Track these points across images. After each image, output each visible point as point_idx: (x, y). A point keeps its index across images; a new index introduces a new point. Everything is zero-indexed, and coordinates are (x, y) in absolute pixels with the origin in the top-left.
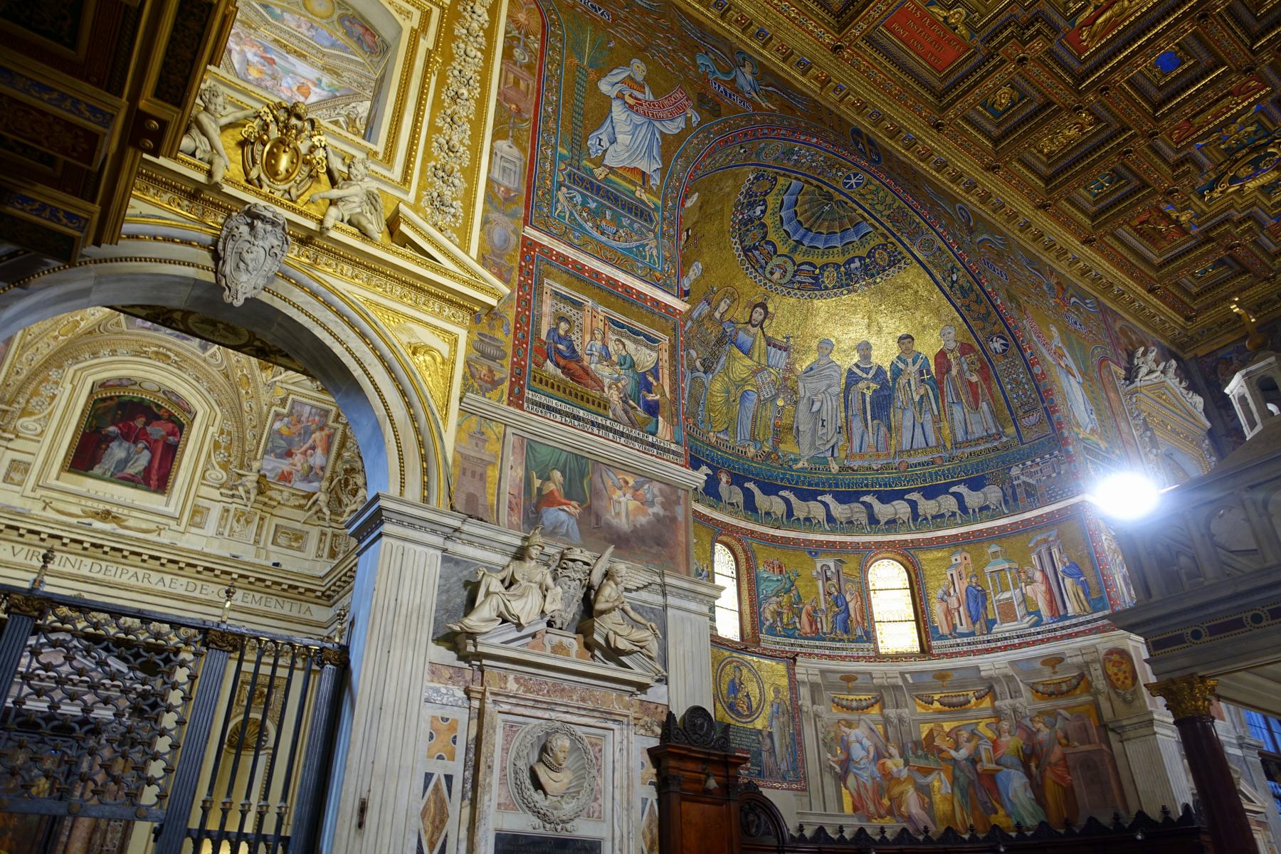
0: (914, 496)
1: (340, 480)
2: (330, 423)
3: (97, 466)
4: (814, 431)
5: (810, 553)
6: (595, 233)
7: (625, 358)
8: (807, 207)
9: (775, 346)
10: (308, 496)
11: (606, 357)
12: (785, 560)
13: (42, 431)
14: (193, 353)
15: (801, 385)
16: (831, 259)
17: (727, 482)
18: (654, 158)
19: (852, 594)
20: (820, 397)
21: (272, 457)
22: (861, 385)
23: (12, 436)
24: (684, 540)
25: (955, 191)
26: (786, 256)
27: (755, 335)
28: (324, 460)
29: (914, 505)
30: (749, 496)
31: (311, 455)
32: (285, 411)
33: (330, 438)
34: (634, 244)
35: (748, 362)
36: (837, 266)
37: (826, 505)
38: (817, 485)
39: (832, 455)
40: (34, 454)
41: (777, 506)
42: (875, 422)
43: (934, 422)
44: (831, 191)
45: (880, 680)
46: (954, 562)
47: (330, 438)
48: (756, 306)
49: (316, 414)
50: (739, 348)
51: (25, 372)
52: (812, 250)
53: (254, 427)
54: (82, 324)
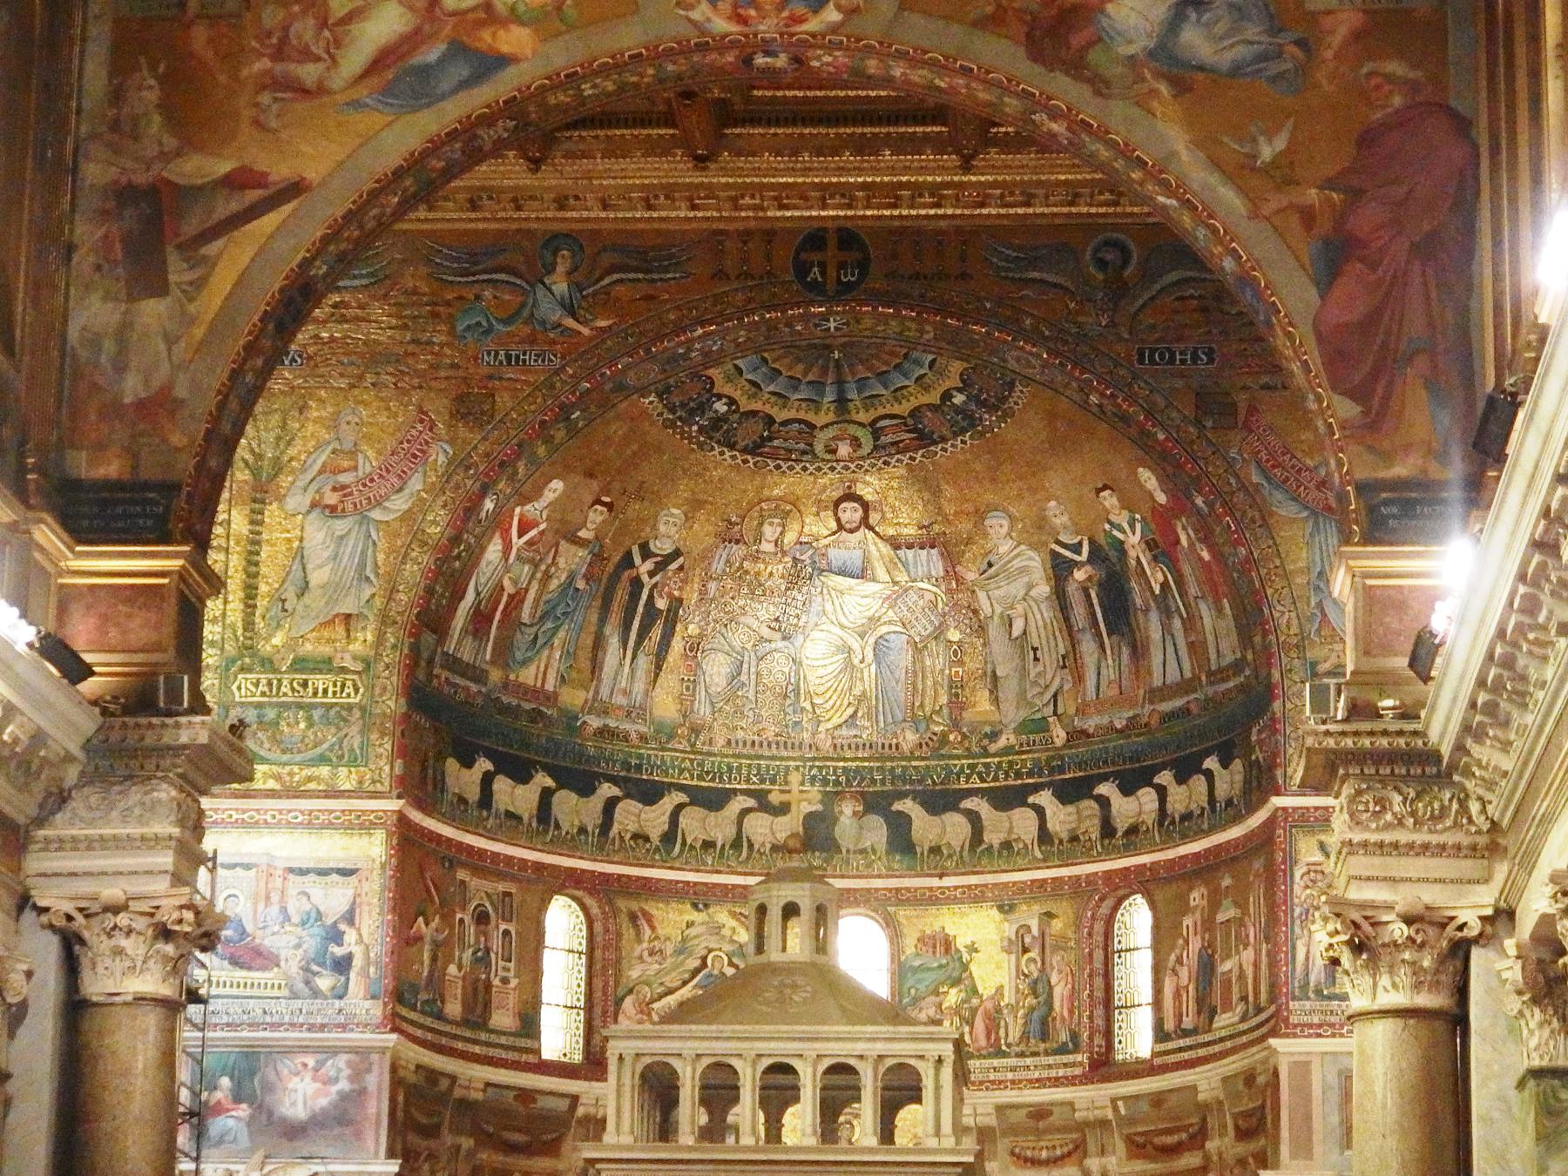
0: (1165, 778)
4: (1023, 672)
5: (1001, 908)
6: (276, 755)
7: (308, 914)
8: (801, 367)
9: (910, 547)
11: (287, 918)
12: (950, 931)
15: (981, 595)
16: (914, 403)
17: (855, 813)
18: (367, 578)
19: (1060, 972)
20: (1020, 608)
22: (1080, 575)
24: (374, 1110)
25: (1089, 215)
29: (1162, 792)
34: (325, 746)
35: (870, 587)
37: (1040, 811)
38: (1030, 774)
39: (1055, 713)
41: (954, 828)
42: (1114, 637)
43: (1185, 630)
45: (1084, 1114)
46: (1192, 903)
48: (837, 504)
50: (842, 572)
52: (876, 401)
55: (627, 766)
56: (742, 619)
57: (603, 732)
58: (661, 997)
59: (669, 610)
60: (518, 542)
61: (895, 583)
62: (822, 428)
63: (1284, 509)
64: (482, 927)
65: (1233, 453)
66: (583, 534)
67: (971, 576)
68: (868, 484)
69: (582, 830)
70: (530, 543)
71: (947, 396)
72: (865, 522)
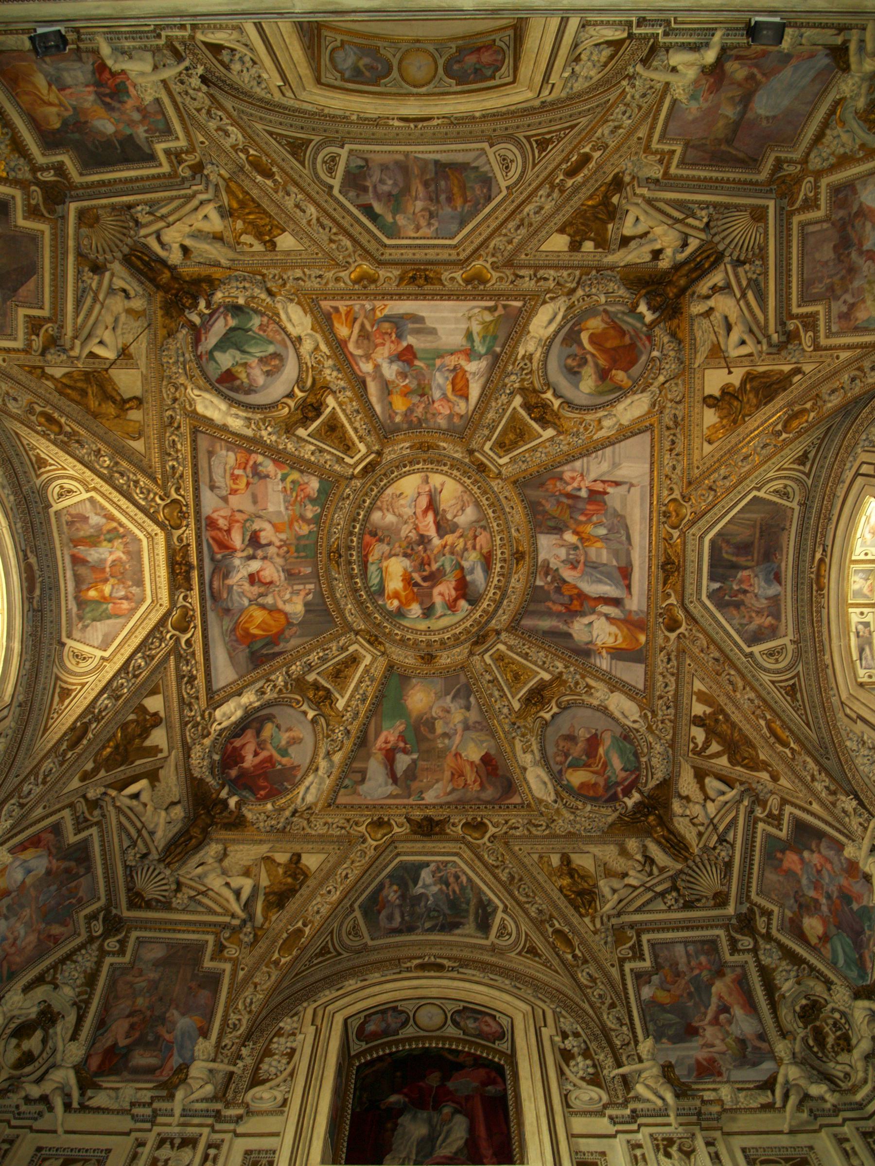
1: (805, 1040)
2: (728, 957)
3: (388, 1157)
10: (769, 1085)
13: (285, 1101)
14: (474, 946)
21: (666, 1044)
23: (240, 1111)
28: (755, 1022)
31: (730, 1022)
32: (647, 964)
33: (742, 983)
40: (277, 1134)
47: (742, 983)
49: (697, 953)
51: (244, 1022)
53: (612, 1006)
54: (307, 930)
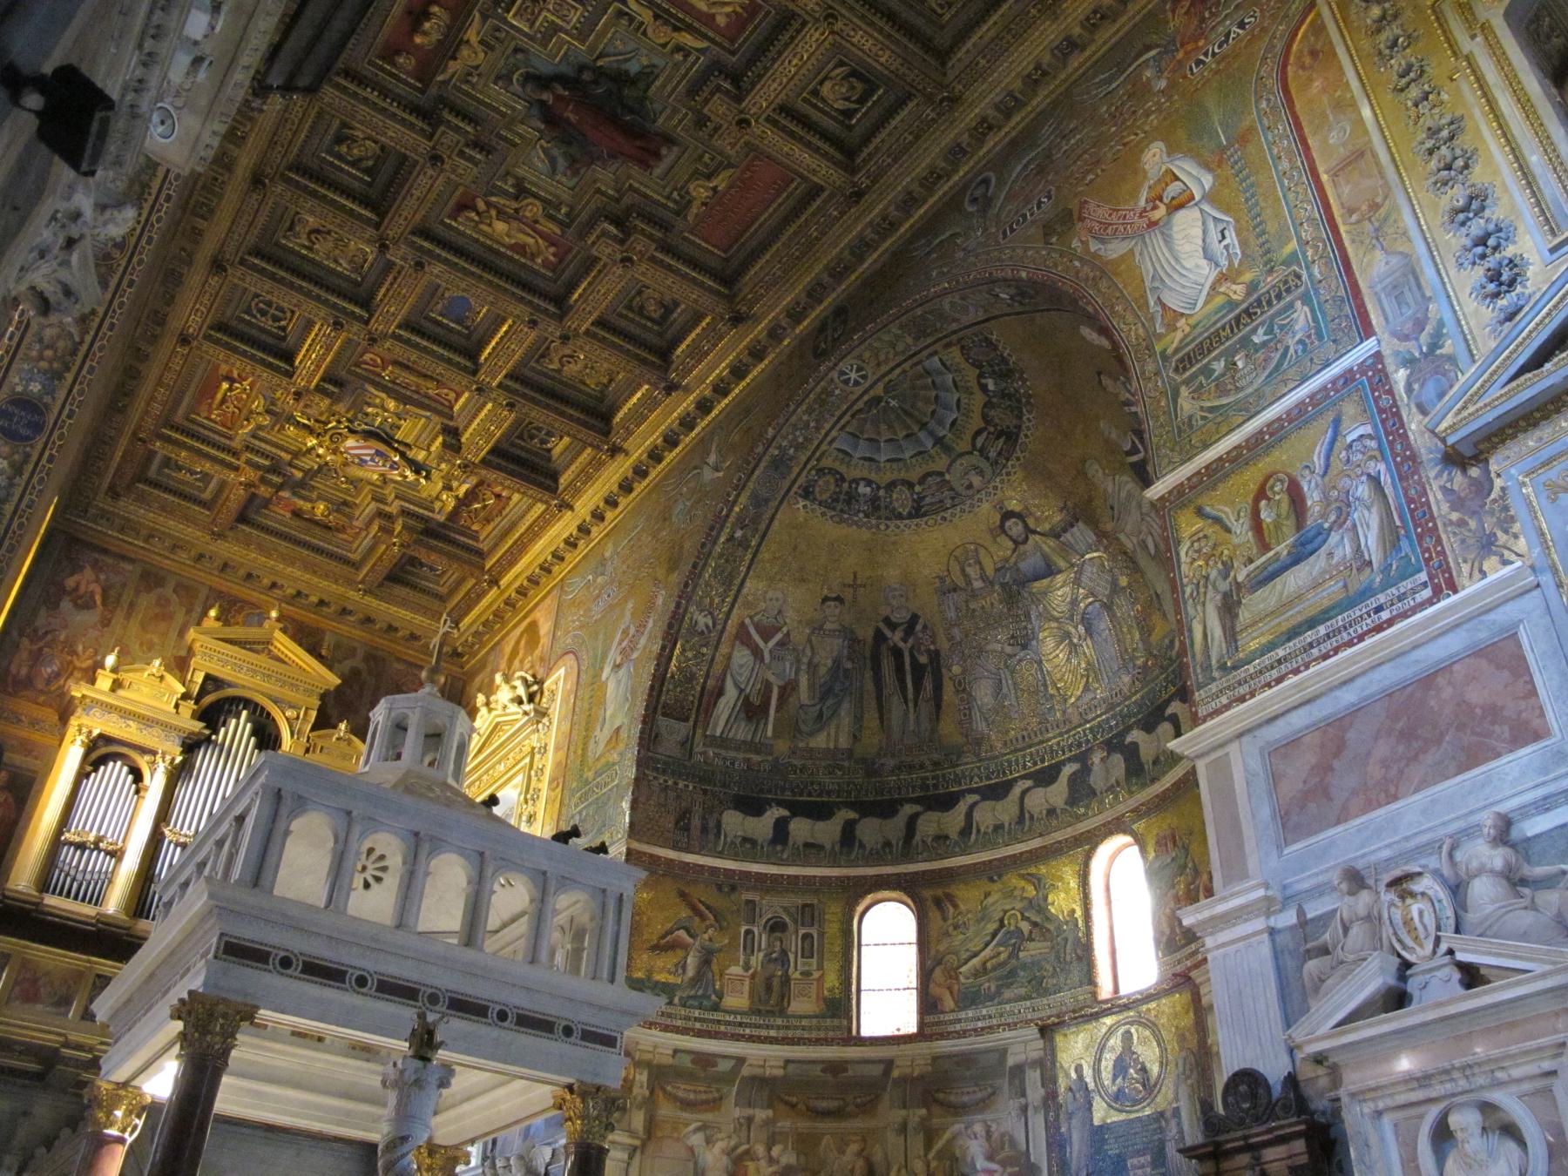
9: (1065, 530)
15: (1122, 537)
26: (953, 461)
27: (1037, 546)
30: (1132, 753)
35: (1060, 578)
36: (988, 405)
44: (866, 398)
50: (1036, 579)
55: (924, 787)
56: (989, 647)
57: (899, 768)
58: (967, 961)
59: (931, 662)
60: (766, 648)
61: (1073, 565)
62: (948, 471)
63: (1114, 250)
64: (778, 934)
65: (1075, 243)
66: (828, 626)
67: (1109, 527)
68: (1011, 498)
69: (888, 844)
70: (781, 644)
71: (984, 388)
72: (1026, 526)
